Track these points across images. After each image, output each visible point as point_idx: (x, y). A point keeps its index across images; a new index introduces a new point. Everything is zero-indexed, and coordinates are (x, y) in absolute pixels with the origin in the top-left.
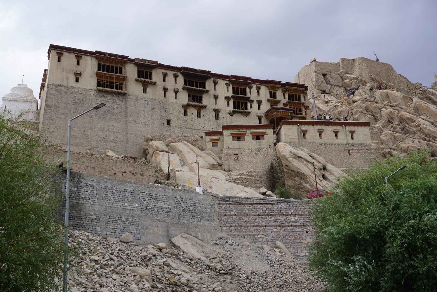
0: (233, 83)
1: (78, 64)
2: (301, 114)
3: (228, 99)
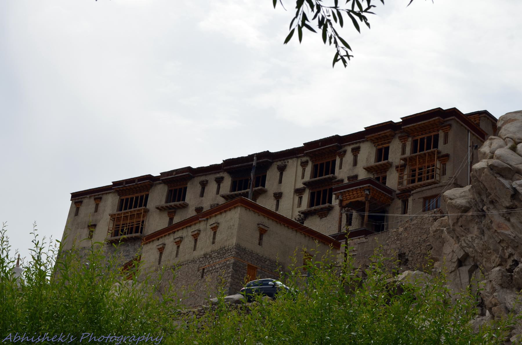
0: (313, 156)
1: (96, 210)
3: (299, 192)
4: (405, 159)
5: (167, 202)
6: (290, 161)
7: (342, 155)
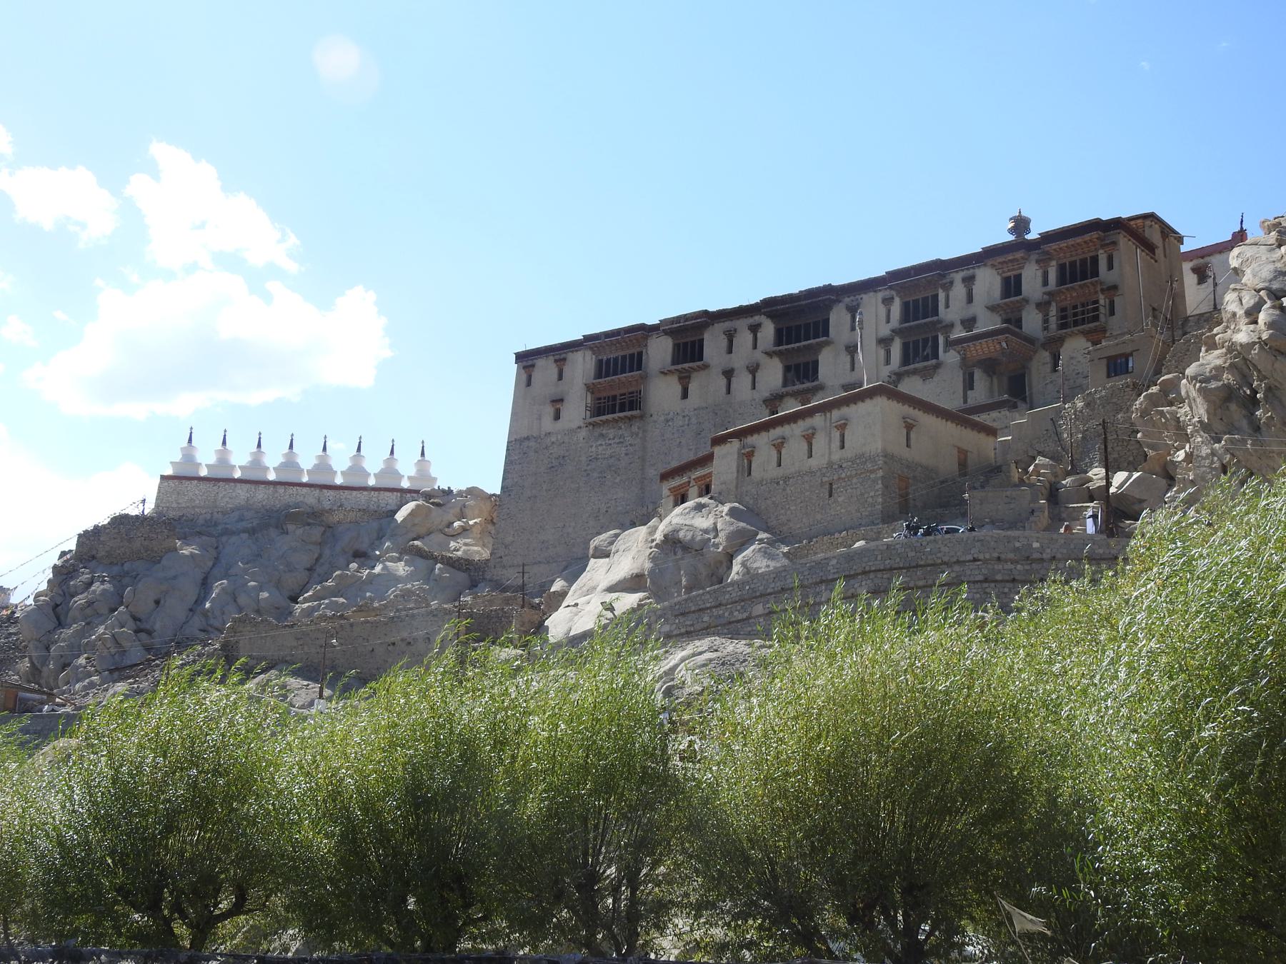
0: (901, 290)
1: (560, 377)
2: (1096, 318)
3: (884, 342)
4: (1049, 293)
5: (673, 363)
6: (864, 296)
7: (948, 286)
